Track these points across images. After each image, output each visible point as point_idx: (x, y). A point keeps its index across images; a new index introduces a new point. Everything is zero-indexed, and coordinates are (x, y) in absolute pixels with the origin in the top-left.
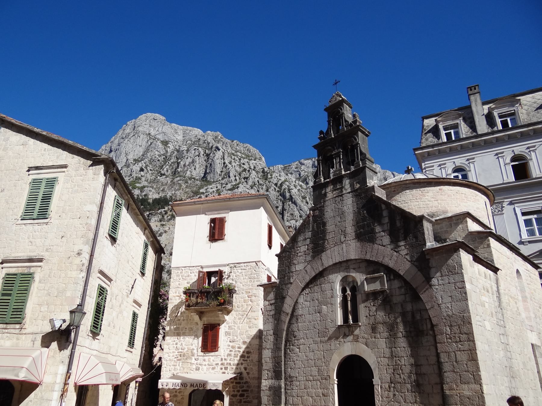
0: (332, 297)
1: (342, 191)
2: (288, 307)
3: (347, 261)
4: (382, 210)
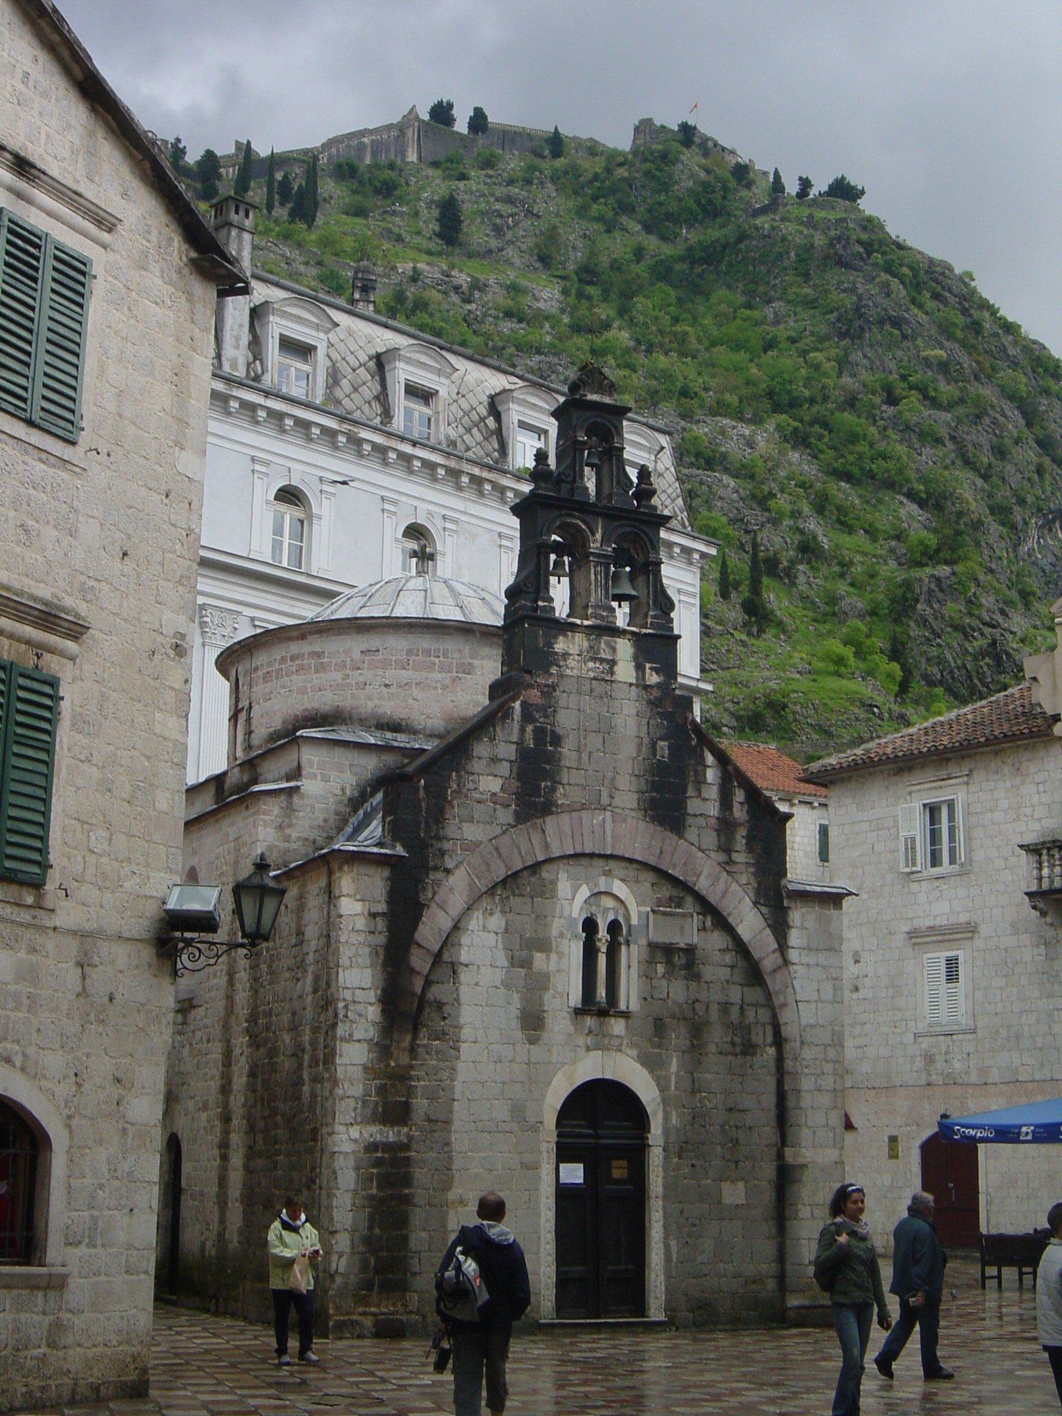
1: (612, 673)
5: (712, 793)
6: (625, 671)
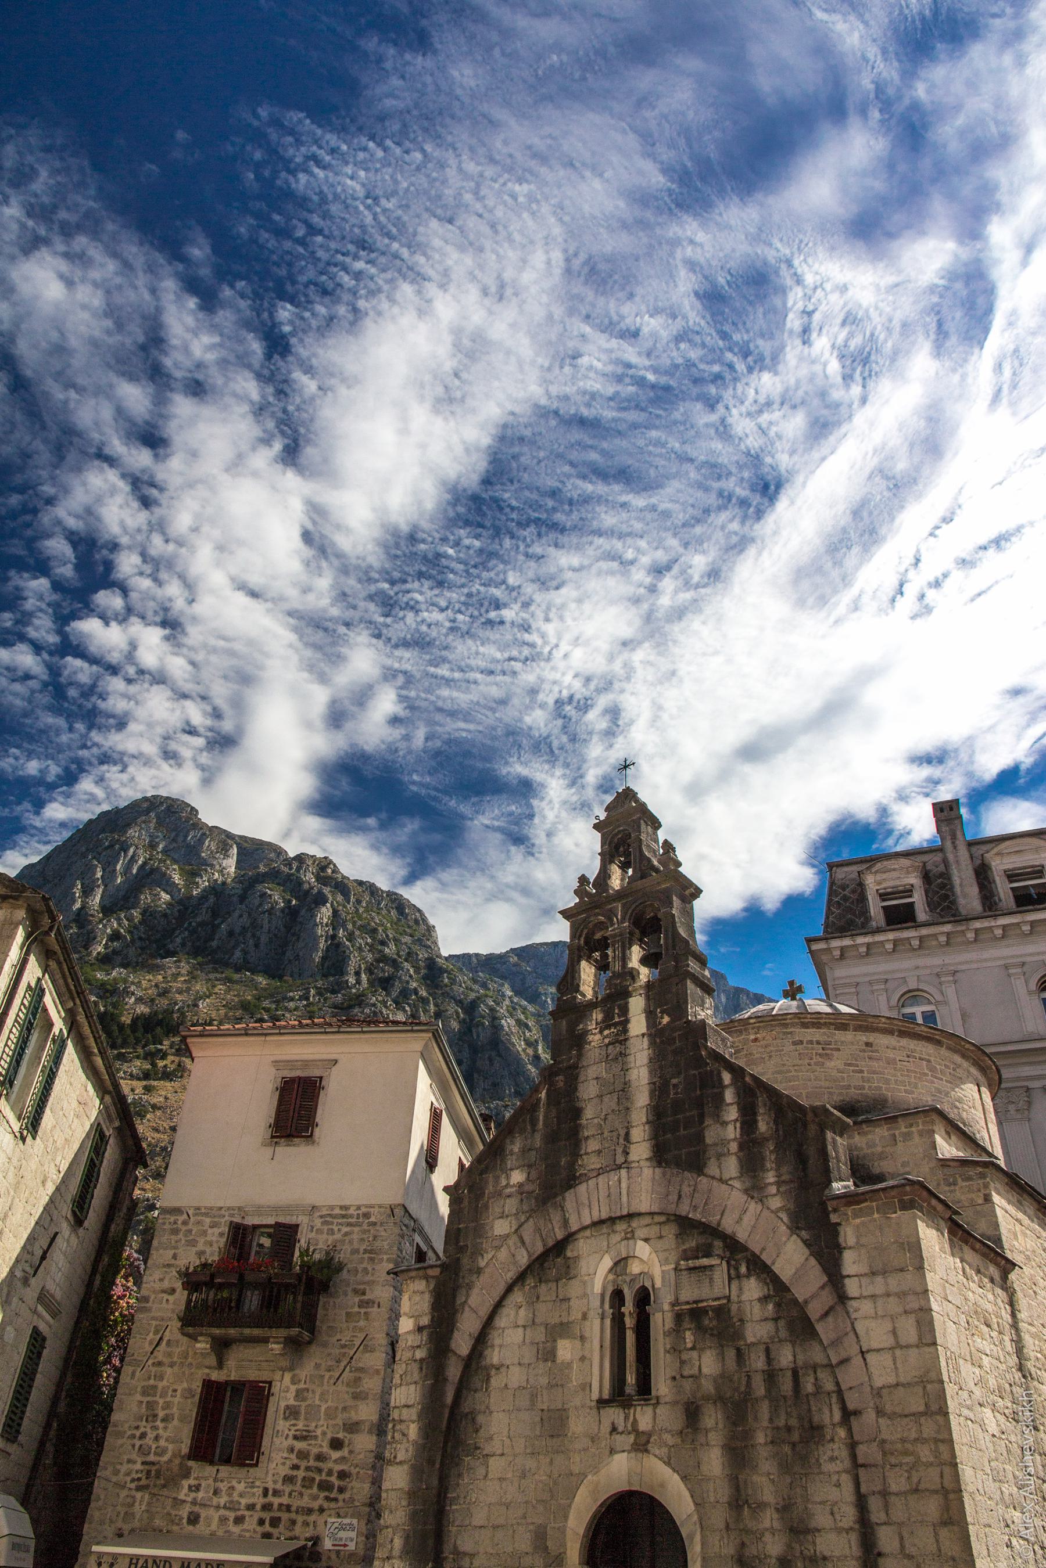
0: (585, 1317)
1: (625, 1031)
2: (461, 1343)
3: (630, 1216)
4: (723, 1087)
5: (732, 1113)
6: (638, 1024)
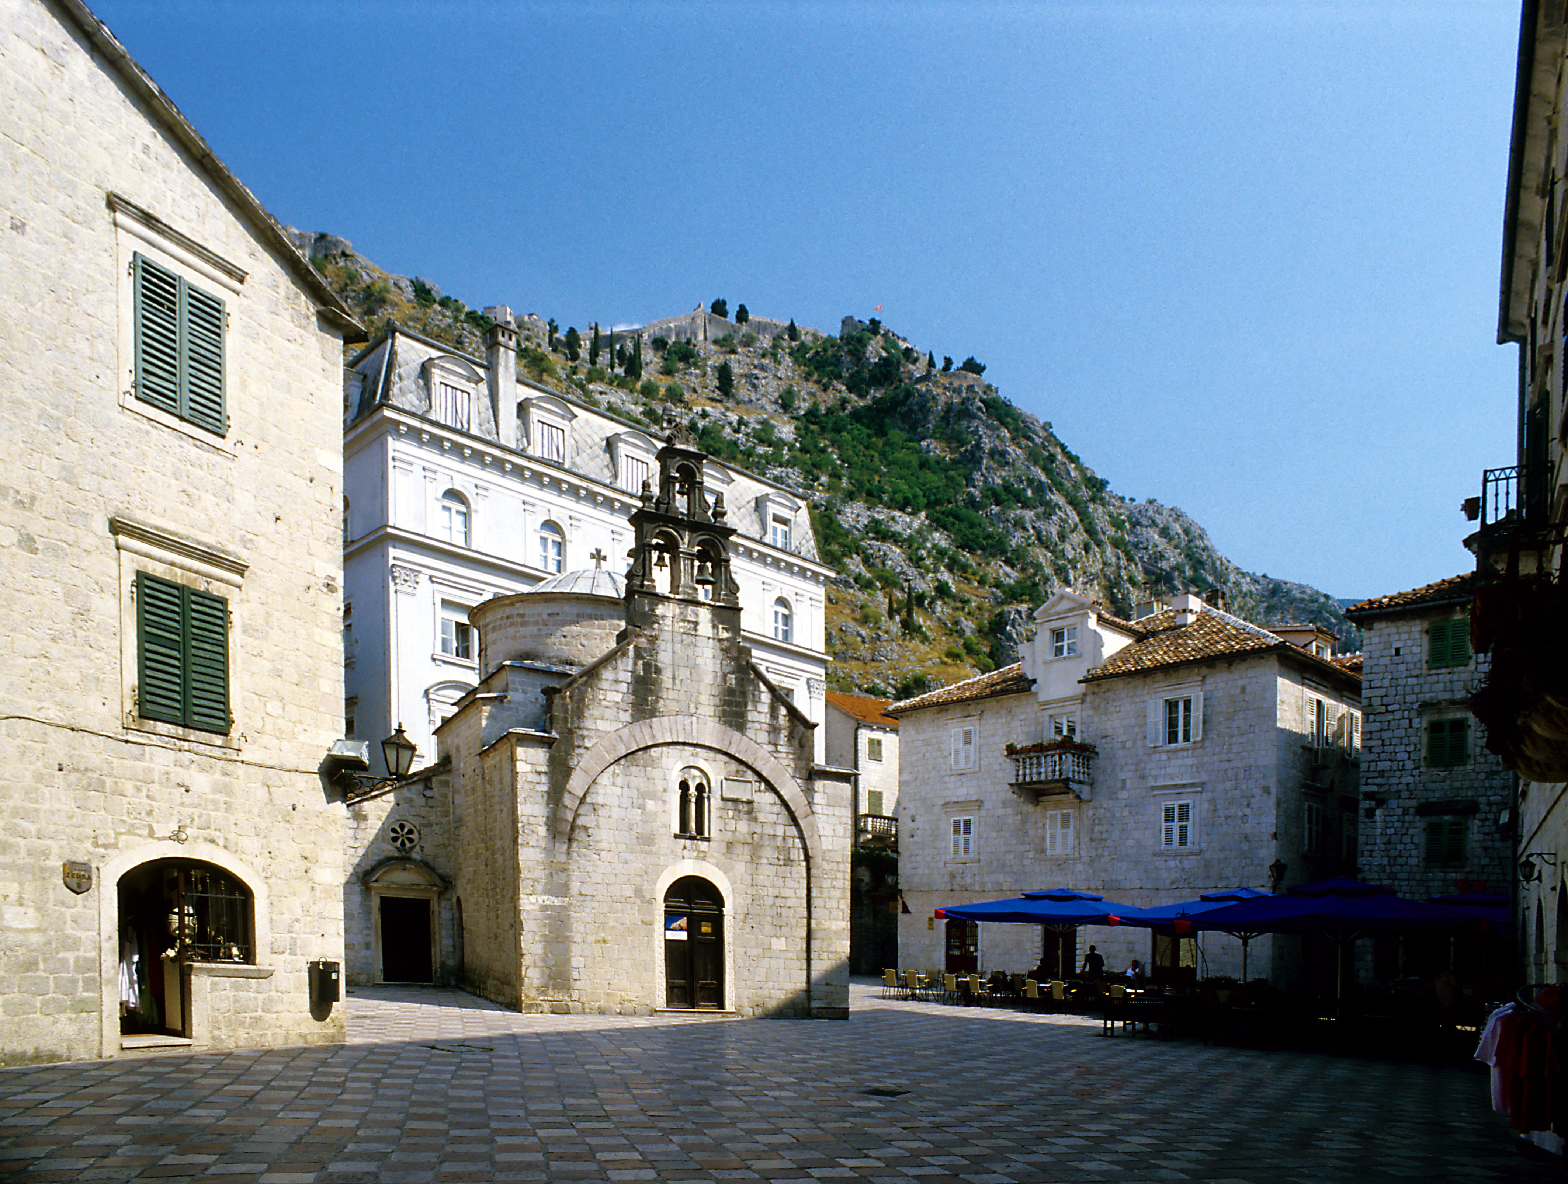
0: (665, 790)
